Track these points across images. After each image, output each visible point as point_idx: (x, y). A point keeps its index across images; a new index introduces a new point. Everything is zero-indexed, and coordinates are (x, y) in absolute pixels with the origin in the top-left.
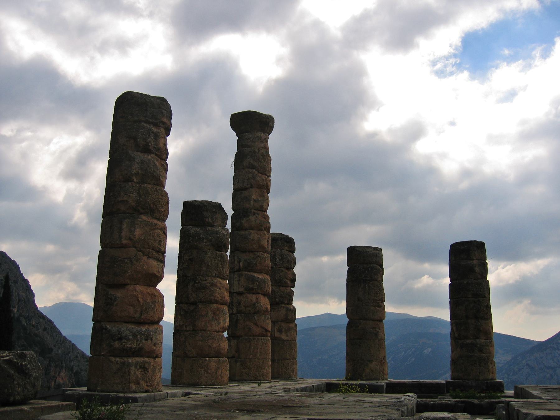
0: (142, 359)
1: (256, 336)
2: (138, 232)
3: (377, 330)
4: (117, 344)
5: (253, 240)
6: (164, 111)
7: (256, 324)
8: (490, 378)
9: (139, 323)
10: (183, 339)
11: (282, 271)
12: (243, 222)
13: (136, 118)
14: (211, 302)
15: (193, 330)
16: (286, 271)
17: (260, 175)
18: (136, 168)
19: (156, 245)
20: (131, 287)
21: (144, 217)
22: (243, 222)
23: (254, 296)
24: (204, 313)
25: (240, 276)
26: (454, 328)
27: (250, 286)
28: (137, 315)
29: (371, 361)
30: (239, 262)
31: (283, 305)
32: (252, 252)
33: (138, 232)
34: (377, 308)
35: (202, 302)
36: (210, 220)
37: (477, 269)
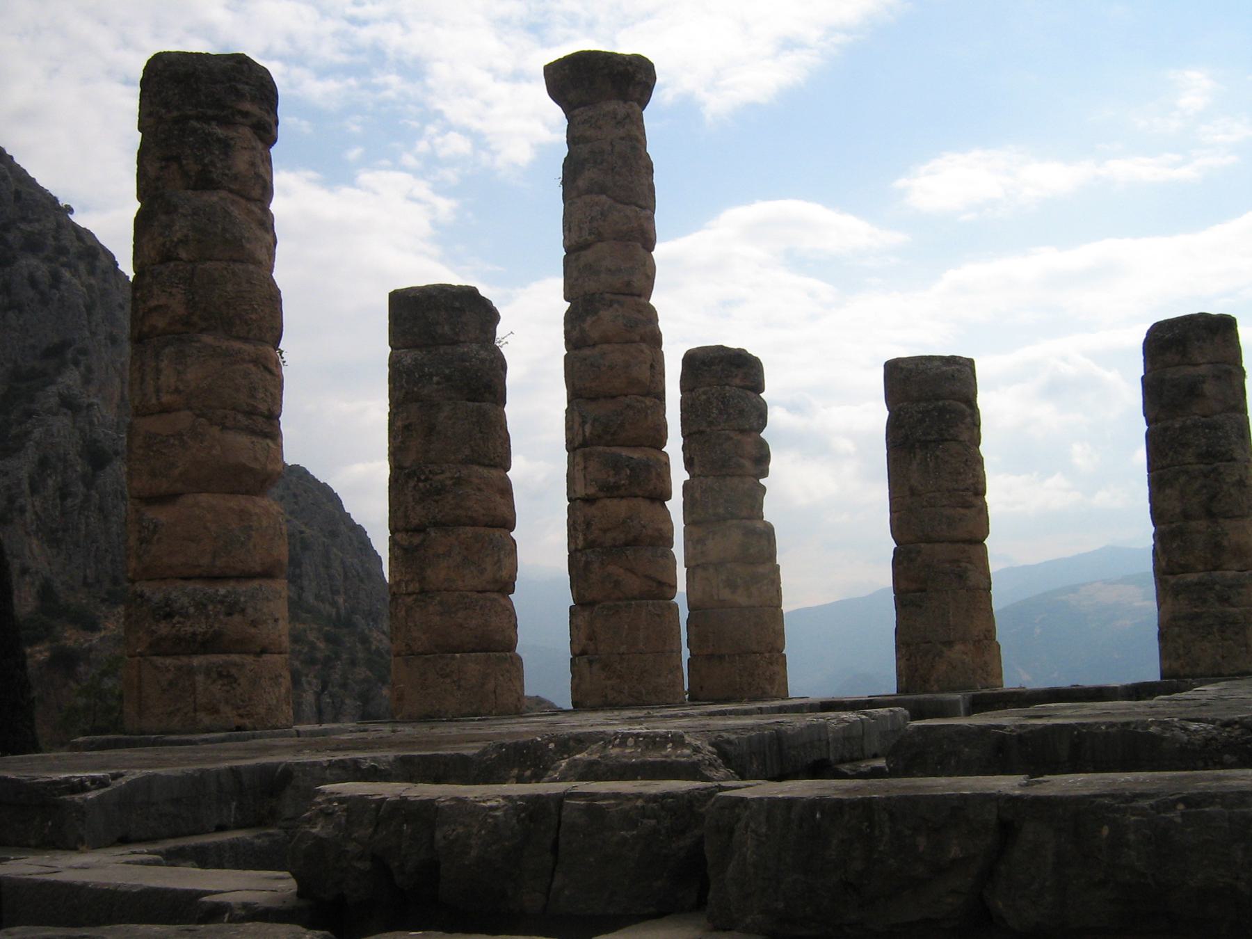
0: (224, 657)
1: (634, 598)
3: (963, 564)
4: (164, 628)
5: (611, 368)
6: (240, 86)
7: (631, 571)
10: (403, 613)
11: (729, 438)
12: (586, 326)
13: (175, 114)
14: (457, 523)
15: (422, 591)
16: (739, 437)
17: (620, 206)
18: (181, 228)
21: (207, 339)
22: (586, 326)
23: (624, 503)
25: (586, 458)
26: (1158, 546)
27: (612, 480)
29: (950, 644)
30: (584, 423)
31: (735, 522)
32: (613, 397)
34: (962, 511)
35: (437, 524)
36: (446, 328)
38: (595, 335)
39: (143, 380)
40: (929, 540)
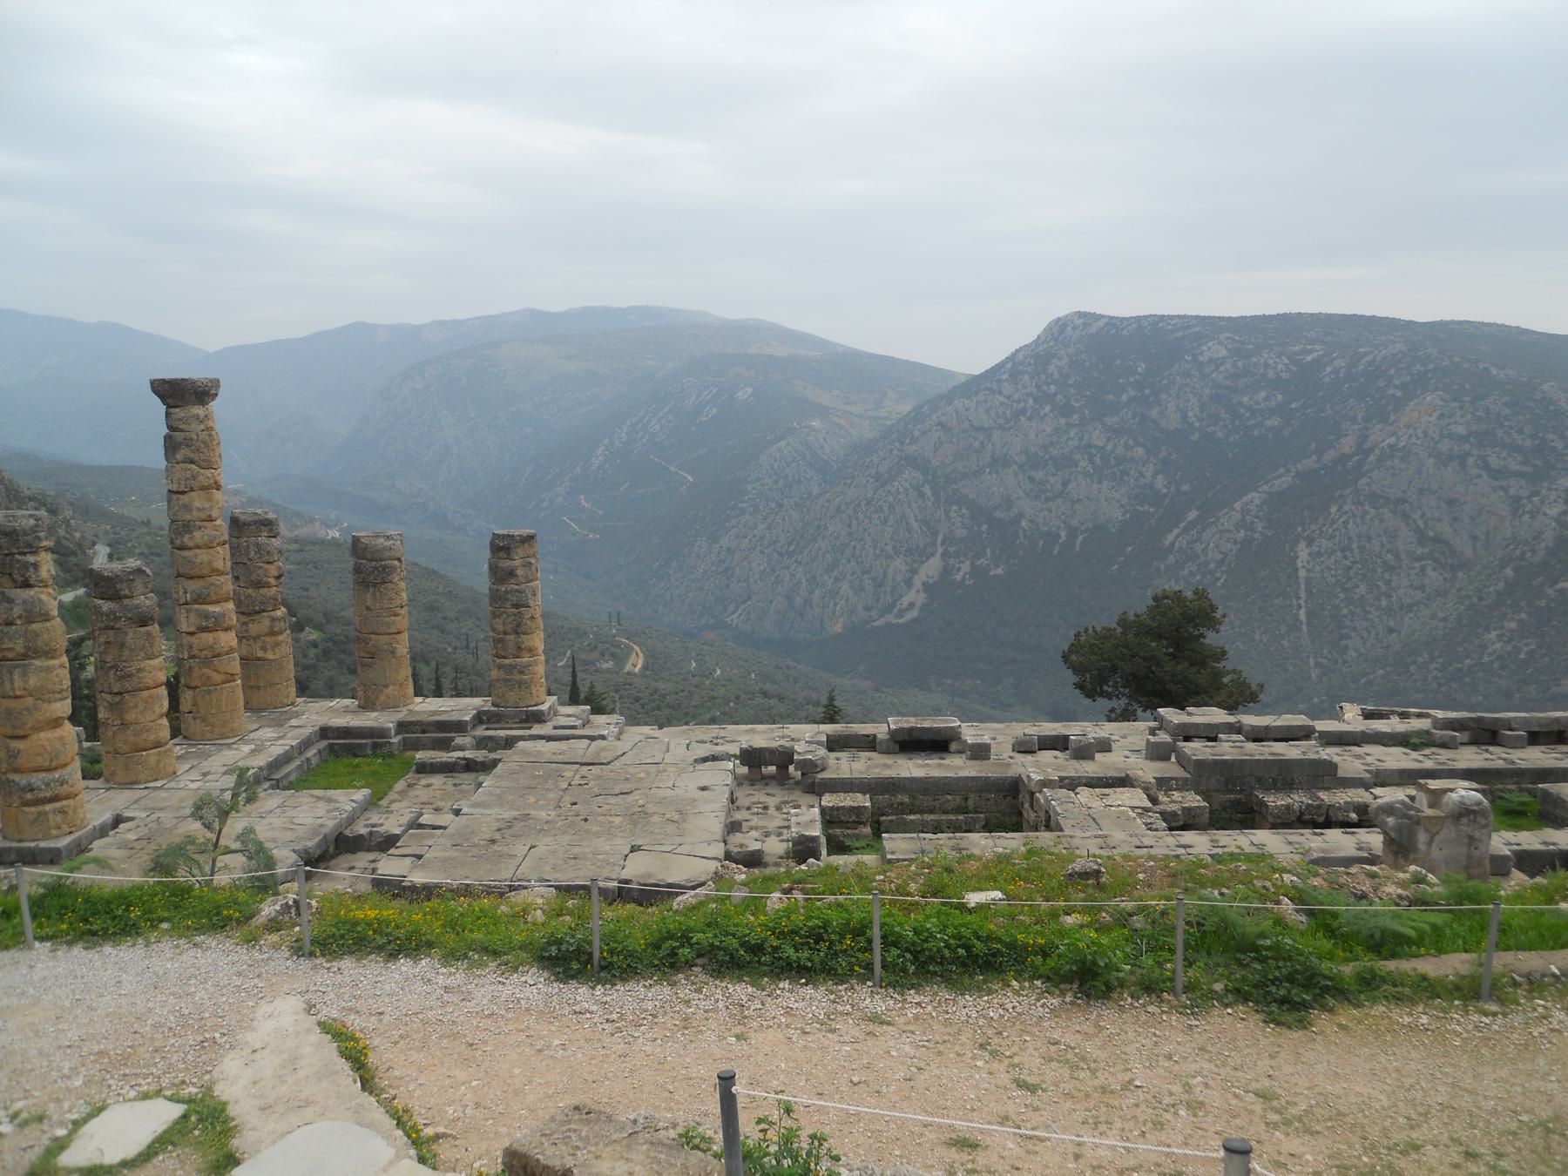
2: (33, 681)
4: (29, 796)
9: (49, 770)
14: (141, 690)
18: (17, 610)
19: (57, 687)
20: (34, 737)
21: (37, 663)
25: (188, 611)
28: (46, 764)
29: (386, 686)
33: (33, 681)
37: (519, 572)
38: (190, 544)
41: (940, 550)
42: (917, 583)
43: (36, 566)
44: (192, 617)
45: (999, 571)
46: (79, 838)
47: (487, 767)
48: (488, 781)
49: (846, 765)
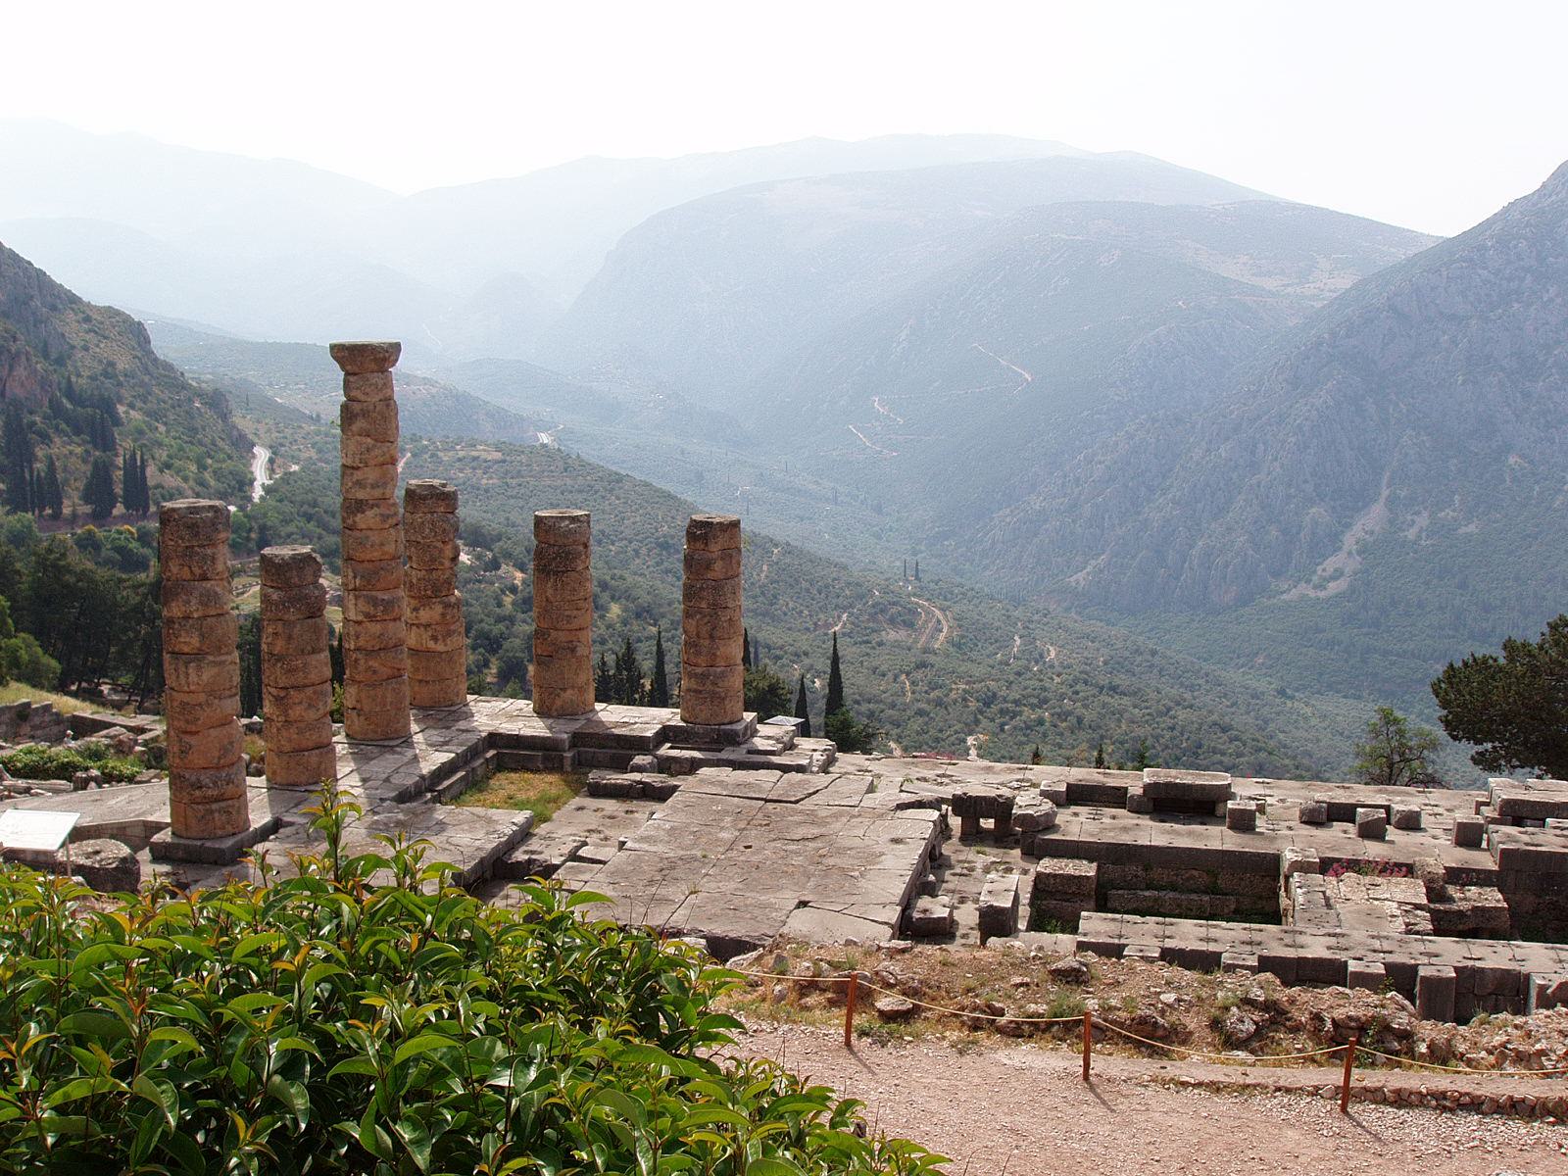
8: (726, 721)
11: (435, 547)
12: (357, 519)
14: (306, 686)
21: (211, 658)
22: (357, 519)
23: (378, 626)
24: (297, 701)
25: (357, 598)
27: (372, 613)
29: (564, 690)
30: (355, 577)
34: (575, 612)
37: (718, 566)
39: (178, 677)
40: (557, 630)
41: (1385, 493)
42: (1349, 541)
43: (214, 559)
44: (361, 602)
45: (1472, 528)
46: (242, 840)
47: (661, 795)
48: (661, 810)
49: (1078, 824)
